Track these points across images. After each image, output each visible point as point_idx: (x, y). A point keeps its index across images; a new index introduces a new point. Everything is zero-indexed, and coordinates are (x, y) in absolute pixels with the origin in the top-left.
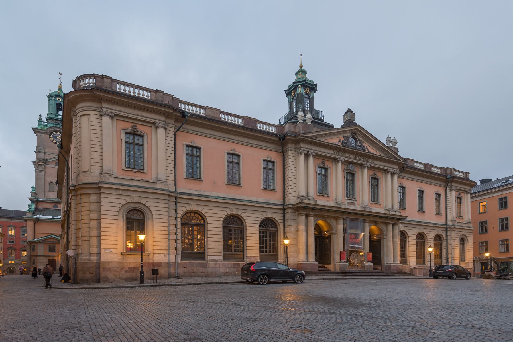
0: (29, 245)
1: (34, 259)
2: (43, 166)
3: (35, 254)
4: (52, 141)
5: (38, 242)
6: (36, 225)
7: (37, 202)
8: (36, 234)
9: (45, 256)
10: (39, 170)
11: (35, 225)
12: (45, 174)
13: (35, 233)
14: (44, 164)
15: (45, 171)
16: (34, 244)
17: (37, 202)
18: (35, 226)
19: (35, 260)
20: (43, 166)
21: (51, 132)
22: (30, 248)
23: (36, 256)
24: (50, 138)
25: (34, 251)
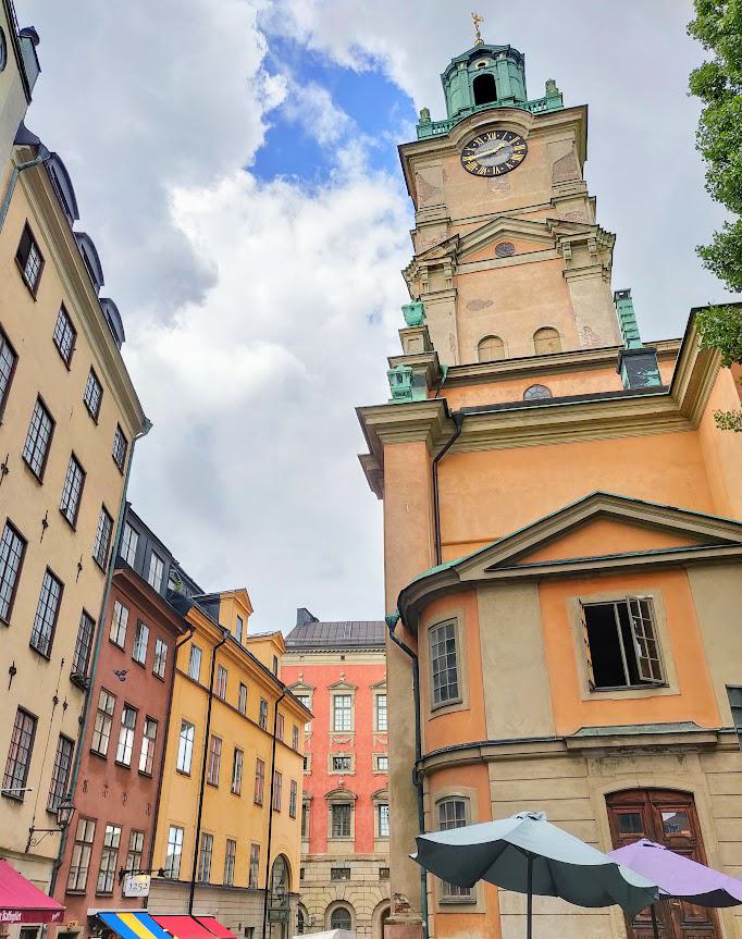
0: (403, 647)
1: (457, 791)
2: (448, 272)
3: (457, 730)
4: (474, 173)
5: (476, 573)
6: (440, 470)
10: (430, 294)
12: (457, 308)
14: (449, 260)
16: (441, 614)
18: (441, 487)
20: (448, 272)
21: (466, 143)
23: (478, 756)
24: (464, 164)
25: (448, 691)
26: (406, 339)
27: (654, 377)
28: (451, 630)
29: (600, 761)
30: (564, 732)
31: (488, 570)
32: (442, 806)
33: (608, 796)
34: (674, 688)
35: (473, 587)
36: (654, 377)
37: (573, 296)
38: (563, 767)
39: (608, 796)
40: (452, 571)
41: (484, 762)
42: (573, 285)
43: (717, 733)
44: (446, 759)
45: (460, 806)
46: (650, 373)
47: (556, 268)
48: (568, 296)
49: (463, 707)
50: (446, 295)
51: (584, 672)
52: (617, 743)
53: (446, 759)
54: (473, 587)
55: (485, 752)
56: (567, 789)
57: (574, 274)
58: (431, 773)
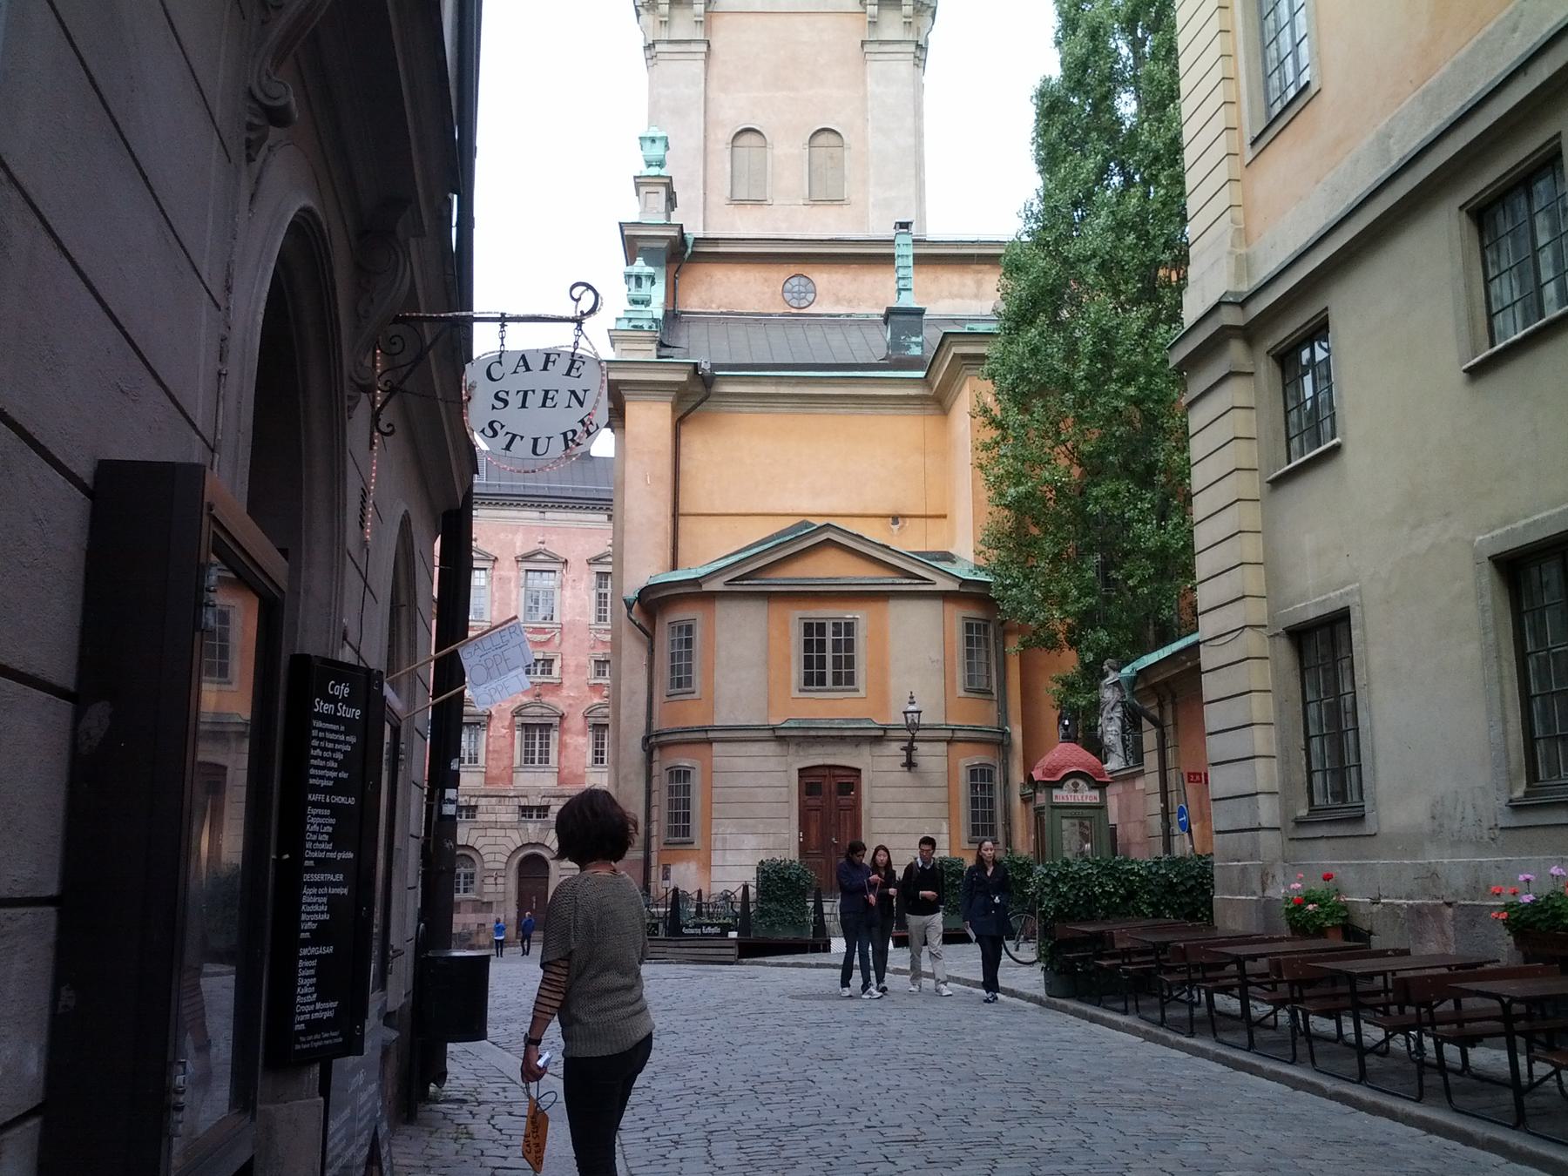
0: (639, 626)
5: (717, 585)
6: (684, 429)
7: (675, 267)
8: (682, 521)
9: (781, 737)
10: (670, 42)
11: (683, 440)
13: (676, 515)
15: (708, 43)
16: (681, 614)
17: (675, 267)
18: (683, 450)
19: (696, 781)
22: (651, 651)
23: (704, 737)
25: (681, 679)
26: (643, 190)
27: (917, 344)
28: (689, 629)
29: (798, 744)
30: (775, 721)
31: (726, 584)
32: (671, 773)
33: (800, 770)
34: (862, 693)
35: (713, 596)
36: (917, 344)
37: (872, 86)
38: (771, 748)
39: (800, 770)
40: (695, 582)
41: (710, 742)
42: (874, 67)
43: (885, 730)
44: (678, 737)
45: (687, 773)
46: (914, 339)
47: (855, 30)
48: (864, 82)
49: (696, 696)
50: (693, 47)
51: (796, 672)
52: (813, 733)
53: (678, 737)
54: (713, 596)
55: (711, 735)
56: (772, 764)
57: (875, 48)
58: (662, 746)
